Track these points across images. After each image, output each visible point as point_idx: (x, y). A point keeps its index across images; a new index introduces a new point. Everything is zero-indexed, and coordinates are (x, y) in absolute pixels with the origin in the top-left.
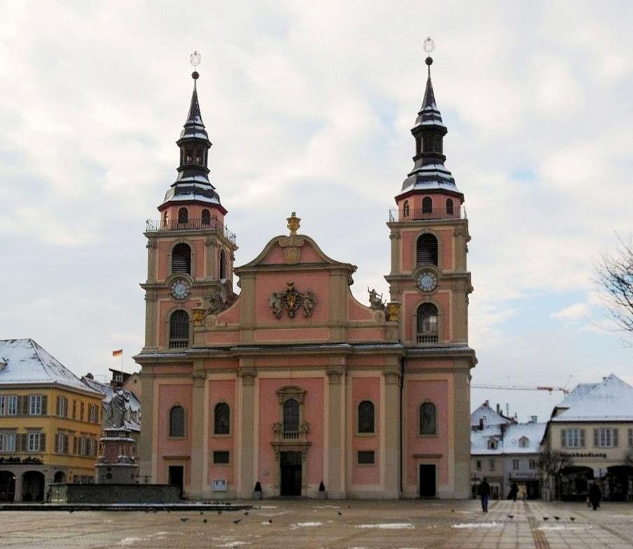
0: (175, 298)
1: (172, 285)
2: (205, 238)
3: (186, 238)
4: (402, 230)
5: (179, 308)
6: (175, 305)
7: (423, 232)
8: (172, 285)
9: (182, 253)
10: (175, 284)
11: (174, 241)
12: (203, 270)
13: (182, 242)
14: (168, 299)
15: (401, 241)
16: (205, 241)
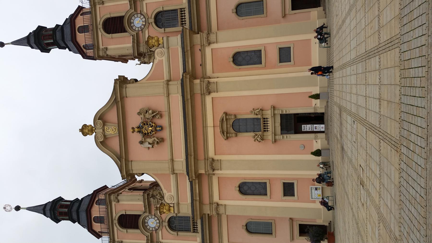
0: (159, 227)
1: (149, 229)
2: (113, 203)
3: (114, 219)
4: (101, 47)
5: (166, 224)
6: (164, 227)
7: (102, 29)
8: (149, 229)
9: (129, 222)
10: (148, 227)
11: (117, 228)
12: (132, 203)
13: (117, 221)
14: (160, 233)
15: (109, 47)
16: (115, 203)
